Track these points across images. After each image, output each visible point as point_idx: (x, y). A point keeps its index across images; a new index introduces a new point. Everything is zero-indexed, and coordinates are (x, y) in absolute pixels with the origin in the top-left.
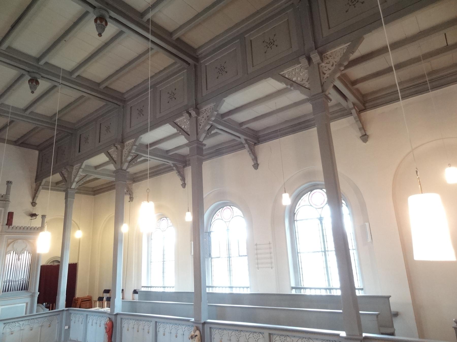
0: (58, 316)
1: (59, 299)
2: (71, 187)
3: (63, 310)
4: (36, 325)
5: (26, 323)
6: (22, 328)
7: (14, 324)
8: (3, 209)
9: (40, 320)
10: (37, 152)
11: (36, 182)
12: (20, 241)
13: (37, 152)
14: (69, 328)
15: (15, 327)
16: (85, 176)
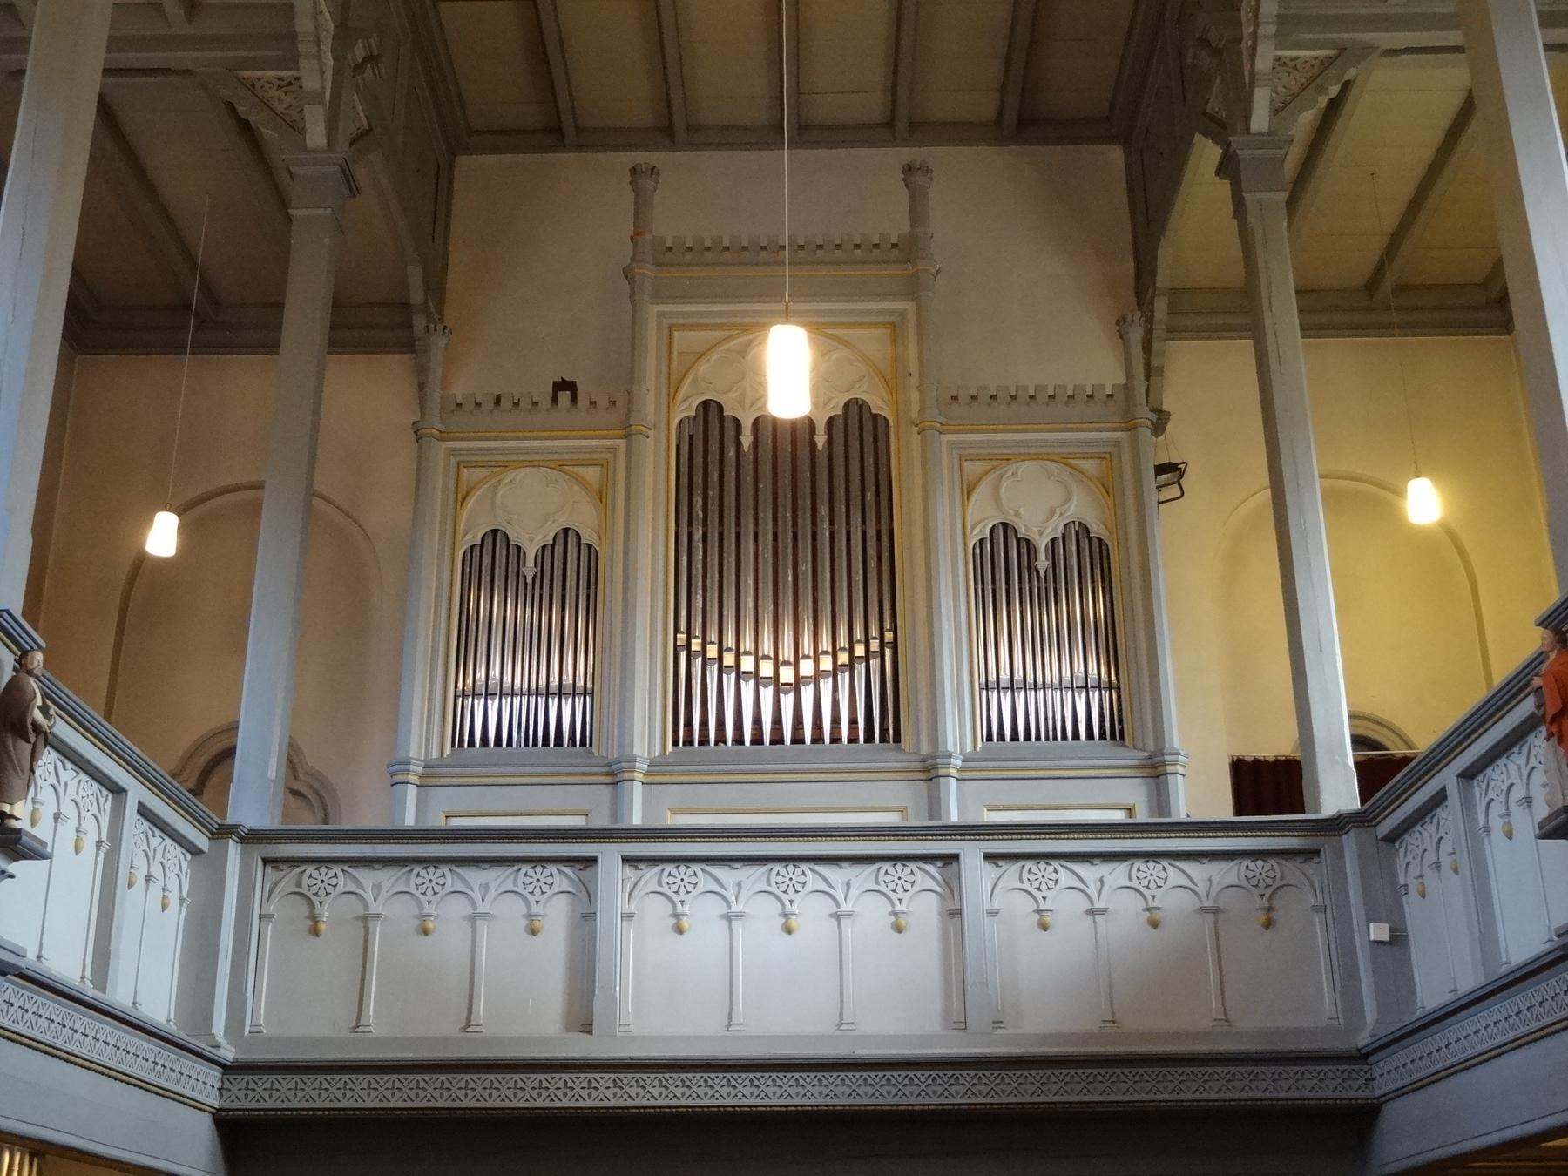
0: (1311, 867)
1: (1316, 786)
2: (1248, 129)
3: (1337, 825)
4: (1177, 888)
5: (1116, 873)
6: (1098, 905)
7: (1045, 870)
8: (909, 306)
9: (1197, 871)
10: (1116, 154)
11: (1140, 305)
12: (1024, 466)
13: (1116, 154)
14: (1398, 939)
15: (1065, 891)
16: (1328, 63)
